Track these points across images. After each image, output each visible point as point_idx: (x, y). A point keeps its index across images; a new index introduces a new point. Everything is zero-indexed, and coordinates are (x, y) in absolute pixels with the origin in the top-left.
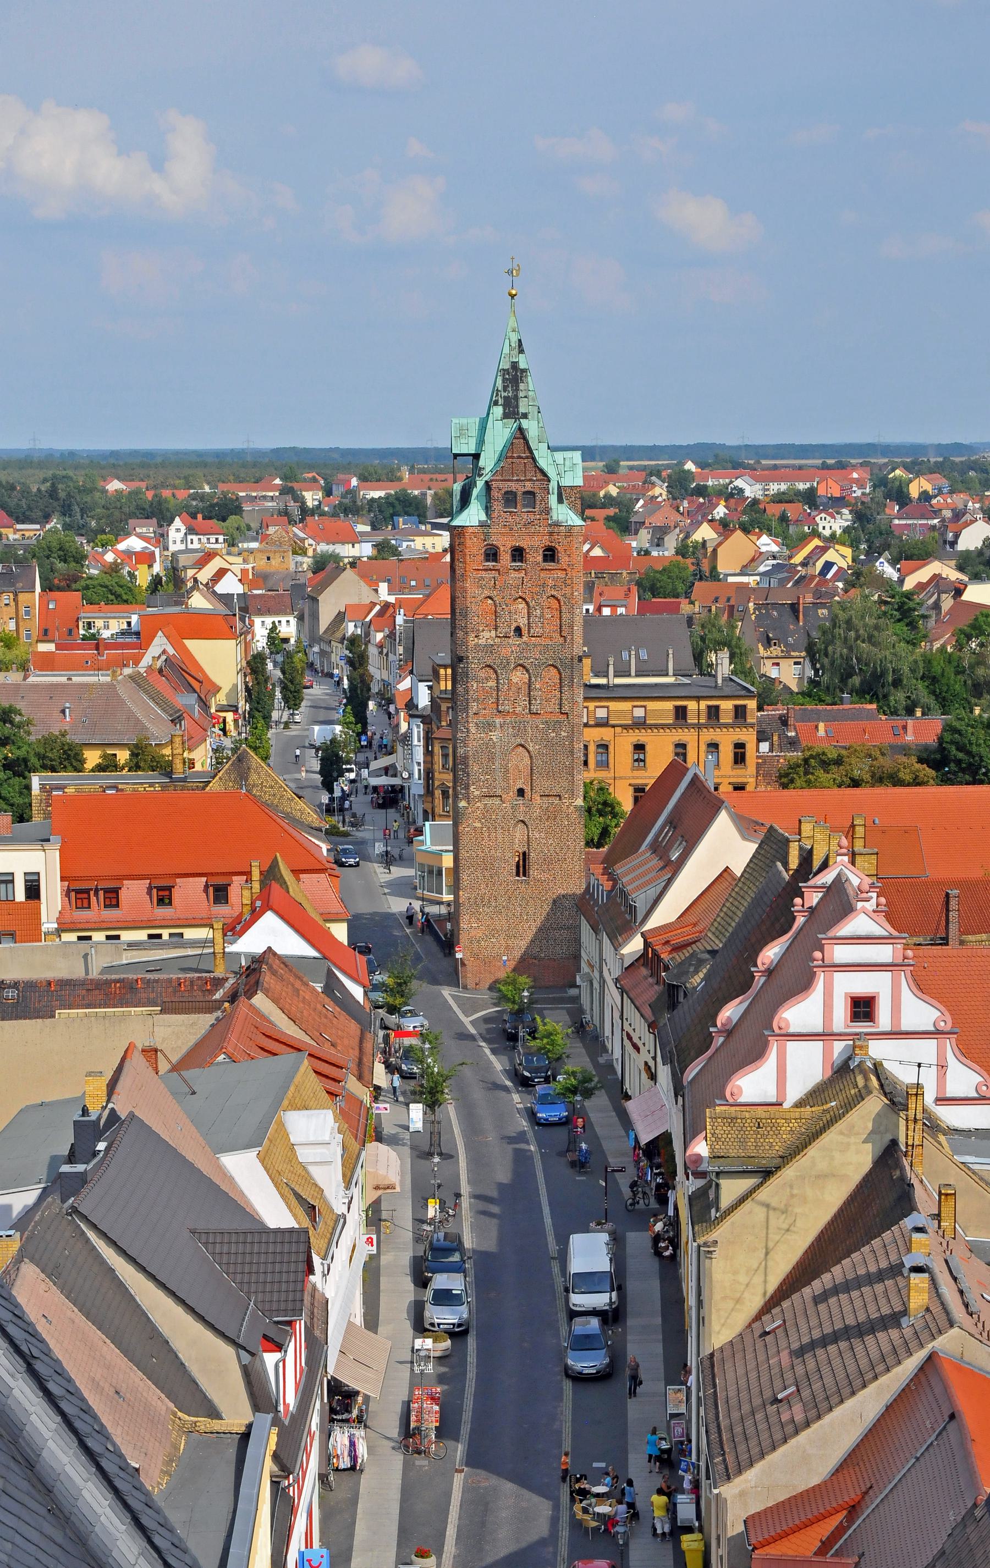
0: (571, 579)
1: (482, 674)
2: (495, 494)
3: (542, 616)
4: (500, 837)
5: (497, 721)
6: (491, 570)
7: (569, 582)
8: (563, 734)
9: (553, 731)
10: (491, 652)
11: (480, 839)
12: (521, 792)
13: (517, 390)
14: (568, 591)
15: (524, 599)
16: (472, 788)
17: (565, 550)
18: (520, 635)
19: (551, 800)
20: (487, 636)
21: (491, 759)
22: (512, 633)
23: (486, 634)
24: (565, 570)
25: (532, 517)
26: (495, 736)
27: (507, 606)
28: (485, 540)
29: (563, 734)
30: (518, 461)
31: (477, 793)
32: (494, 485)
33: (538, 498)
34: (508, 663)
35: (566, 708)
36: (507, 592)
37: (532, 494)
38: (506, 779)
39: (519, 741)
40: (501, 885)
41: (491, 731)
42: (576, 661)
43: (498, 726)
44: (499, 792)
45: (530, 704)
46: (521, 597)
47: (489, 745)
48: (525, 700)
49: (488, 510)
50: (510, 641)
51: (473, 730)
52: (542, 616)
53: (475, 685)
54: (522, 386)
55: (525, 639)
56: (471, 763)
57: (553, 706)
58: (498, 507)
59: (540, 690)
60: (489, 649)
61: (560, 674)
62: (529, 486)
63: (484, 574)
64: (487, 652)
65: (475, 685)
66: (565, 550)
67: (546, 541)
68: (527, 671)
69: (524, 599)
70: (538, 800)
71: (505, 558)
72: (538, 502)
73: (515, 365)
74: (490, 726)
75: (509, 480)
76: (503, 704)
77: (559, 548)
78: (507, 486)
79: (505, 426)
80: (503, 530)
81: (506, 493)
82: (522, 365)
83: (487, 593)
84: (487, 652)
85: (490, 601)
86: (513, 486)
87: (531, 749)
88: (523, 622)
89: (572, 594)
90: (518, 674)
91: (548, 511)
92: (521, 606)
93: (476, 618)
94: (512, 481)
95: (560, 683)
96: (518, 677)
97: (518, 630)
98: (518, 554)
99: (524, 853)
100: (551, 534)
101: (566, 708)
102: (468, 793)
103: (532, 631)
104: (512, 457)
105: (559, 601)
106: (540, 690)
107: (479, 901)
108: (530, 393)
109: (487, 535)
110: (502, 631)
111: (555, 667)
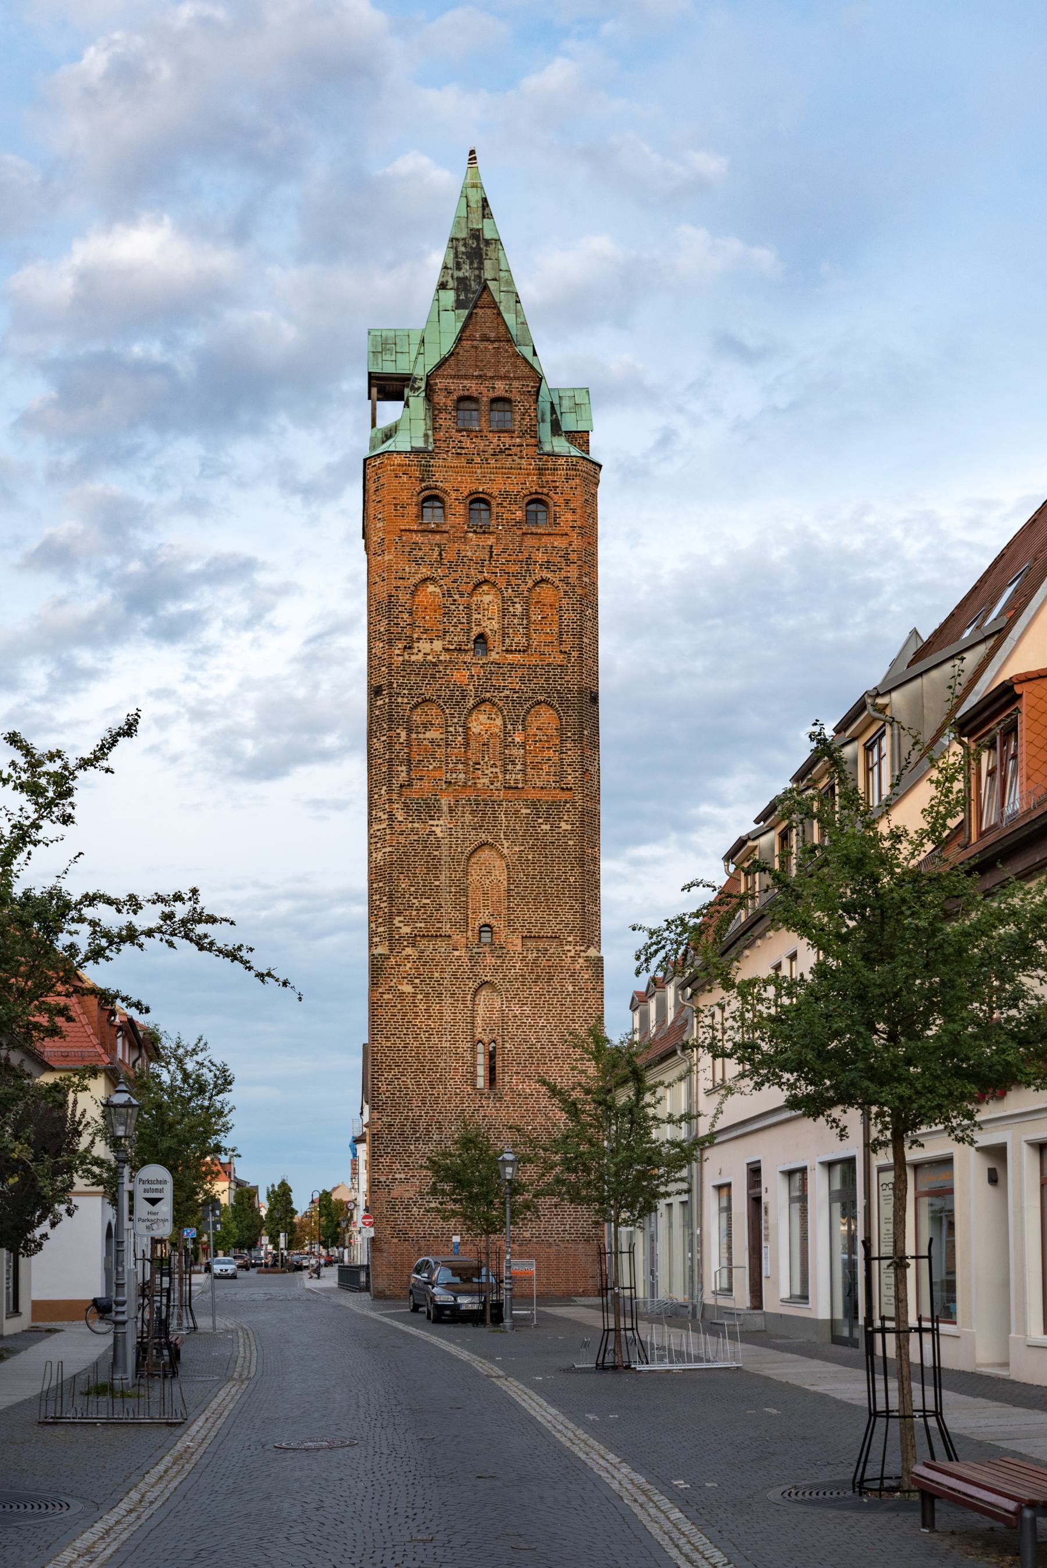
3: (526, 614)
4: (448, 1016)
8: (564, 826)
9: (546, 822)
10: (433, 676)
13: (481, 268)
15: (494, 585)
17: (567, 501)
18: (487, 651)
19: (541, 945)
21: (434, 867)
22: (471, 645)
23: (424, 646)
25: (508, 441)
26: (440, 827)
27: (462, 595)
28: (422, 480)
29: (564, 826)
30: (482, 345)
32: (440, 383)
34: (464, 697)
36: (460, 573)
39: (483, 837)
40: (449, 1101)
41: (432, 818)
43: (445, 808)
44: (447, 929)
45: (505, 772)
46: (486, 581)
47: (429, 842)
48: (494, 765)
51: (400, 816)
52: (526, 614)
53: (403, 735)
54: (487, 264)
55: (494, 656)
56: (395, 874)
60: (431, 668)
62: (500, 388)
63: (418, 538)
64: (425, 676)
66: (567, 501)
67: (532, 483)
69: (494, 585)
71: (457, 514)
73: (476, 234)
74: (429, 809)
75: (466, 377)
78: (460, 387)
79: (458, 317)
80: (455, 462)
81: (462, 399)
82: (488, 235)
83: (425, 571)
84: (425, 676)
85: (431, 588)
86: (473, 387)
87: (505, 851)
88: (491, 625)
90: (483, 718)
91: (532, 432)
92: (487, 599)
93: (406, 616)
104: (472, 338)
108: (502, 274)
109: (426, 471)
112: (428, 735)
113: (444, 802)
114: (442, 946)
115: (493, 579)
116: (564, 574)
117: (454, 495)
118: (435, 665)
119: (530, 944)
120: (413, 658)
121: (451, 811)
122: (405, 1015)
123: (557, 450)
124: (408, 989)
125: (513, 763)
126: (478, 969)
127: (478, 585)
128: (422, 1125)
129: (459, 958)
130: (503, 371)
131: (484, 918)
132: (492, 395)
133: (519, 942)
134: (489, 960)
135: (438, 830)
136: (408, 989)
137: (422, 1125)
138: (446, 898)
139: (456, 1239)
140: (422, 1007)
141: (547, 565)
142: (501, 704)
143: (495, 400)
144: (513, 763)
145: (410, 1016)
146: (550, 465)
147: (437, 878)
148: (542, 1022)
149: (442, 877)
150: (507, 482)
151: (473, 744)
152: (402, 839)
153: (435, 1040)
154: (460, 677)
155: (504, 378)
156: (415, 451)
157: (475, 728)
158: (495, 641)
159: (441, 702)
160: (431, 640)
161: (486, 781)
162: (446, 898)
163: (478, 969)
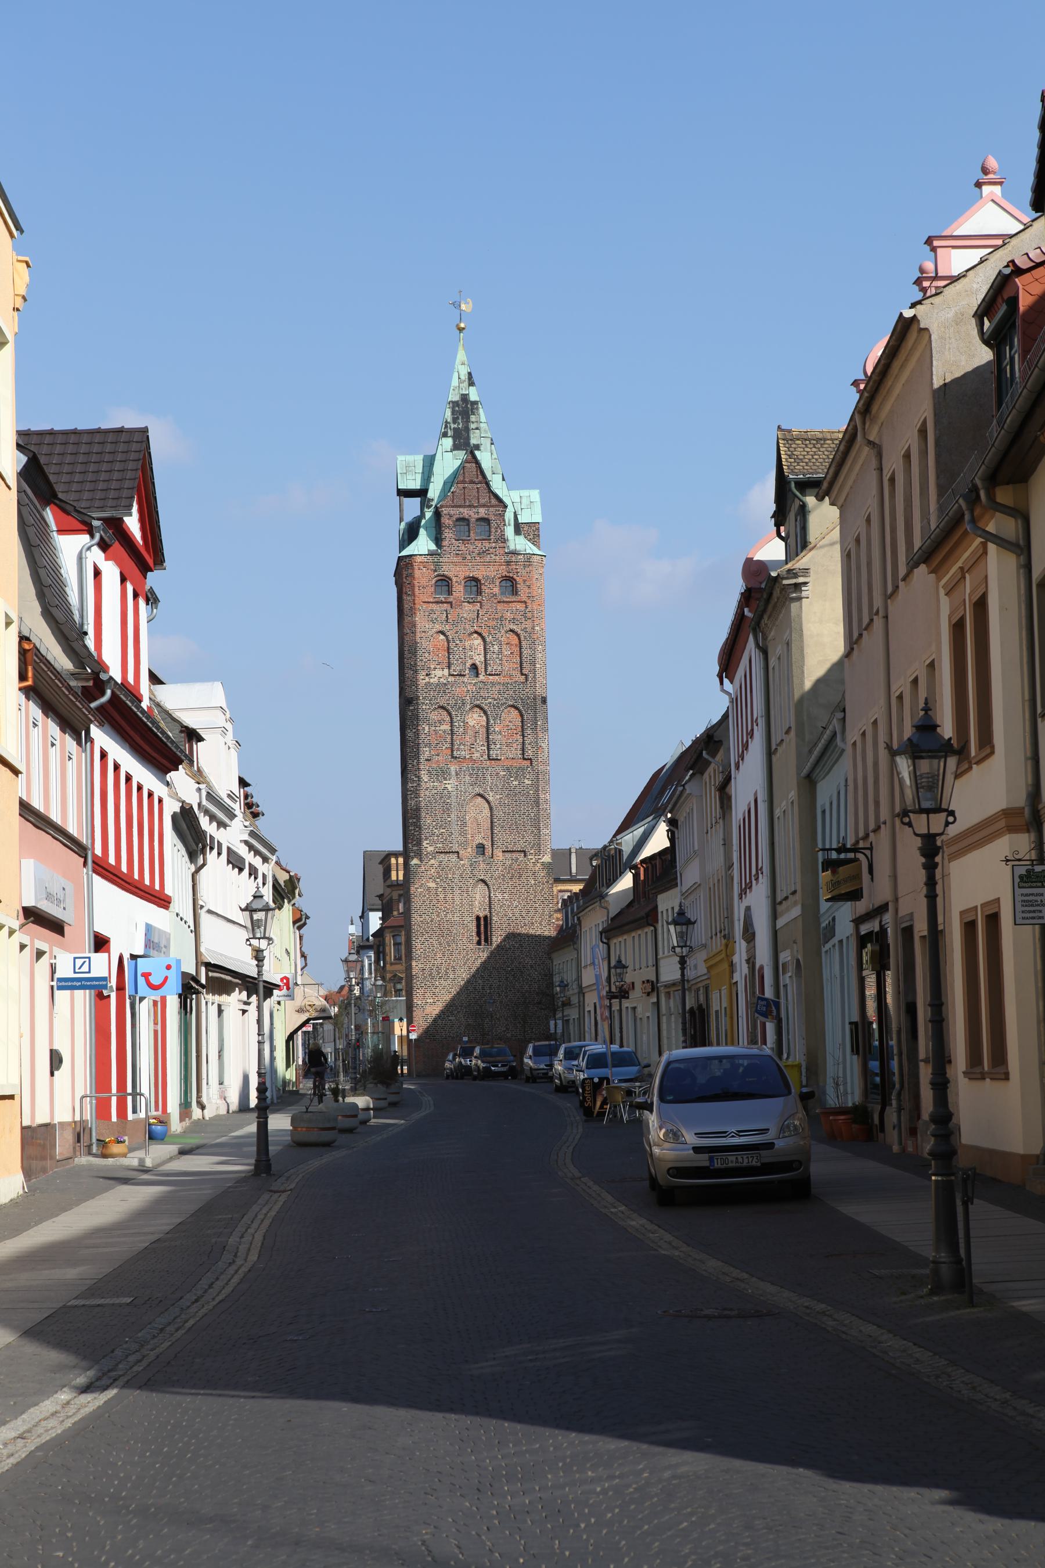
0: (532, 612)
1: (434, 716)
2: (445, 520)
3: (500, 652)
5: (453, 768)
6: (442, 602)
7: (529, 615)
10: (444, 692)
11: (435, 902)
12: (481, 848)
14: (528, 624)
15: (480, 634)
16: (425, 843)
17: (525, 581)
18: (477, 675)
19: (515, 855)
20: (440, 674)
21: (447, 810)
22: (467, 672)
23: (439, 673)
24: (525, 602)
25: (487, 545)
26: (451, 785)
27: (461, 641)
28: (435, 571)
30: (470, 486)
31: (430, 849)
32: (445, 511)
33: (493, 524)
34: (463, 704)
35: (529, 753)
36: (460, 627)
37: (486, 521)
38: (463, 833)
39: (478, 790)
41: (445, 779)
42: (539, 702)
43: (453, 773)
44: (455, 848)
45: (489, 749)
46: (476, 632)
48: (483, 745)
49: (438, 540)
50: (465, 679)
51: (425, 778)
52: (500, 652)
53: (427, 728)
55: (482, 677)
56: (423, 815)
57: (515, 752)
58: (448, 534)
59: (500, 733)
60: (442, 687)
61: (522, 716)
62: (482, 512)
63: (434, 606)
64: (439, 692)
65: (427, 728)
66: (525, 581)
67: (503, 571)
68: (485, 713)
69: (480, 634)
70: (499, 854)
72: (493, 530)
74: (443, 774)
75: (460, 506)
76: (458, 749)
77: (518, 579)
78: (456, 512)
80: (455, 559)
81: (458, 520)
84: (439, 692)
85: (442, 637)
86: (466, 512)
87: (491, 799)
88: (479, 659)
89: (533, 629)
90: (475, 716)
93: (427, 655)
94: (464, 507)
95: (522, 727)
96: (475, 719)
97: (474, 667)
98: (474, 583)
99: (486, 917)
100: (508, 563)
101: (529, 753)
102: (420, 850)
103: (489, 669)
104: (464, 482)
105: (518, 635)
106: (500, 733)
107: (435, 973)
109: (437, 564)
110: (456, 668)
111: (517, 708)
112: (443, 727)
113: (453, 769)
114: (453, 858)
115: (479, 631)
116: (523, 626)
117: (454, 579)
118: (445, 684)
119: (507, 854)
120: (432, 681)
121: (457, 774)
122: (431, 901)
123: (518, 548)
124: (432, 885)
125: (495, 744)
126: (475, 872)
127: (471, 634)
128: (443, 969)
129: (463, 865)
130: (482, 501)
131: (479, 840)
132: (476, 516)
133: (501, 854)
134: (482, 866)
135: (449, 787)
136: (432, 885)
137: (443, 969)
138: (455, 829)
139: (465, 1039)
140: (442, 896)
141: (513, 620)
142: (486, 708)
143: (478, 520)
144: (495, 744)
145: (435, 902)
146: (513, 559)
147: (449, 816)
148: (515, 903)
149: (452, 816)
150: (489, 571)
151: (470, 732)
152: (427, 793)
153: (449, 916)
154: (458, 691)
155: (484, 506)
156: (431, 554)
157: (471, 722)
158: (481, 668)
159: (449, 707)
160: (443, 669)
161: (478, 755)
162: (455, 829)
163: (475, 872)
